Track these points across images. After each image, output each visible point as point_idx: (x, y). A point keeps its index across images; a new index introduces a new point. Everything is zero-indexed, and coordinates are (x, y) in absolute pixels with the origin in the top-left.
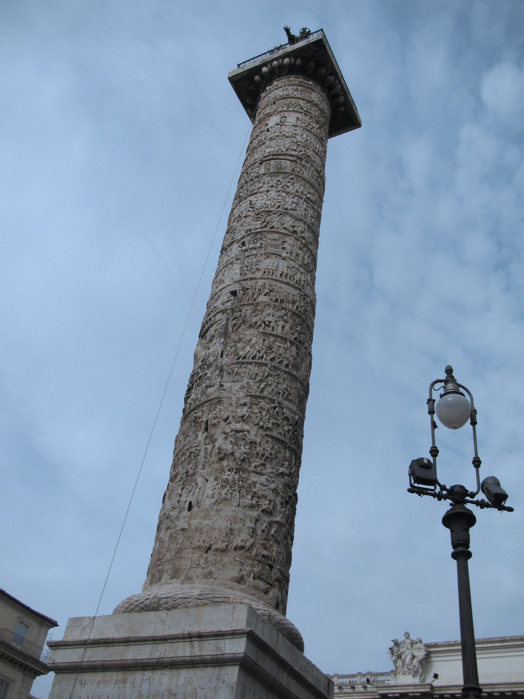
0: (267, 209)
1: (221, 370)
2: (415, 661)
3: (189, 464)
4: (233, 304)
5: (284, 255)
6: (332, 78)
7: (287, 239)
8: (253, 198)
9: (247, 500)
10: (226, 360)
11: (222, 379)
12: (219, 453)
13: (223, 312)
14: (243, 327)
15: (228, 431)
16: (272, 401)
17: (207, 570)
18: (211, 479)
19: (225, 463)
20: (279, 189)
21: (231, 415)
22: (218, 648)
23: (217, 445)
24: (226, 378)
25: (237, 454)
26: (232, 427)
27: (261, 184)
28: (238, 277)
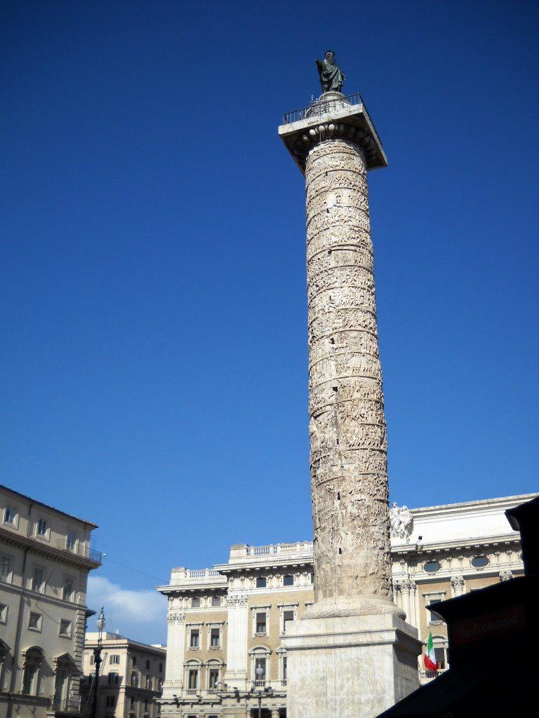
0: (344, 307)
1: (340, 455)
2: (402, 526)
3: (333, 522)
4: (337, 399)
5: (363, 351)
6: (367, 139)
7: (362, 334)
8: (330, 293)
9: (372, 544)
10: (342, 447)
11: (342, 461)
12: (351, 516)
13: (331, 405)
14: (348, 419)
15: (353, 501)
16: (374, 474)
17: (358, 590)
18: (349, 533)
19: (355, 522)
20: (350, 285)
21: (353, 489)
23: (349, 511)
24: (344, 461)
25: (361, 516)
26: (356, 498)
27: (335, 279)
28: (335, 375)
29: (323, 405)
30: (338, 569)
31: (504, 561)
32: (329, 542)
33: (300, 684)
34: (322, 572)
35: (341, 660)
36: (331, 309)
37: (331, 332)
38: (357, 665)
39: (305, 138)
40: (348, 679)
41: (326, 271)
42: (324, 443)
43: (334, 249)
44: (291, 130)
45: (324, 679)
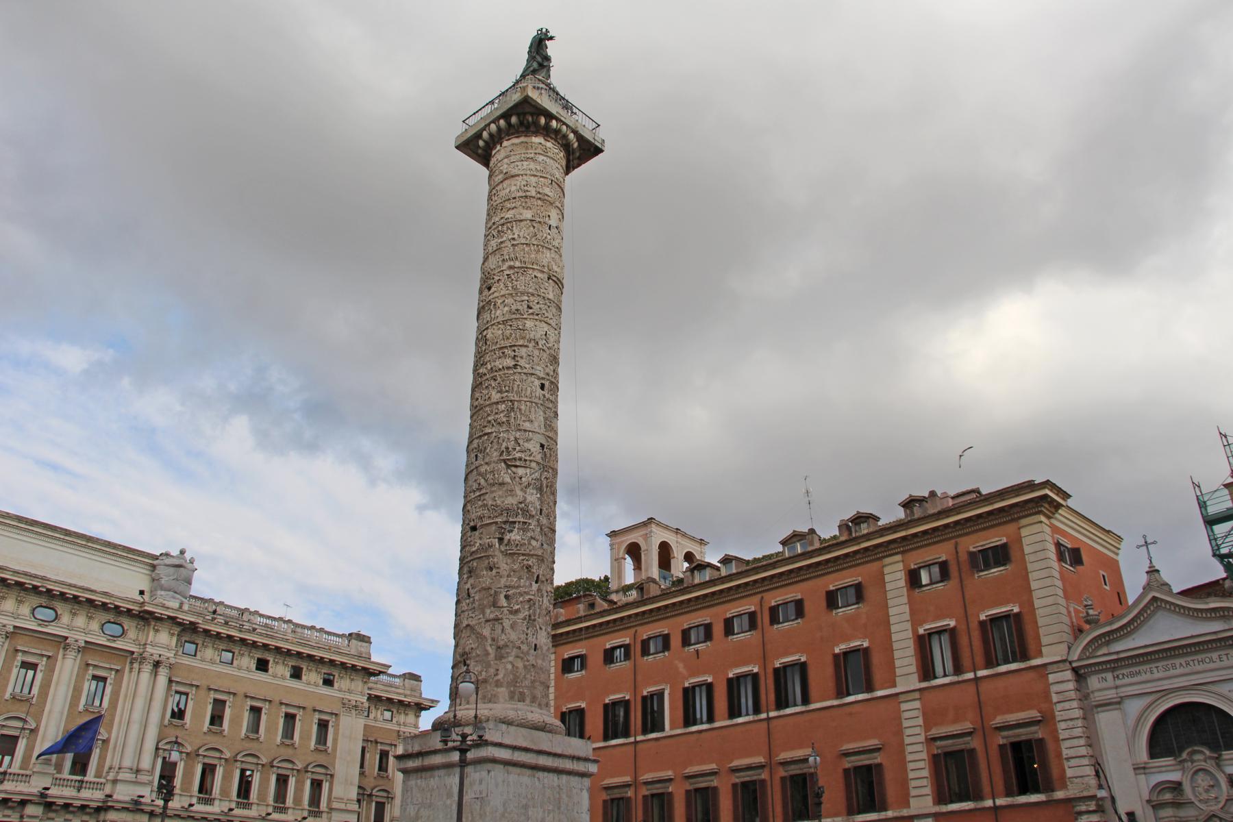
1: (541, 529)
8: (546, 328)
10: (544, 521)
13: (538, 463)
22: (585, 767)
29: (527, 458)
30: (532, 670)
31: (79, 625)
32: (523, 631)
33: (501, 809)
34: (509, 667)
35: (544, 787)
36: (545, 348)
37: (542, 375)
38: (558, 796)
39: (543, 121)
40: (549, 813)
41: (544, 298)
42: (523, 505)
43: (554, 278)
44: (539, 101)
45: (526, 807)
